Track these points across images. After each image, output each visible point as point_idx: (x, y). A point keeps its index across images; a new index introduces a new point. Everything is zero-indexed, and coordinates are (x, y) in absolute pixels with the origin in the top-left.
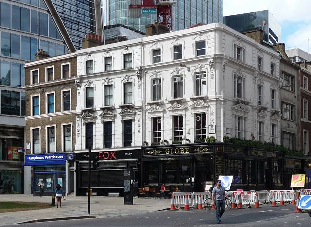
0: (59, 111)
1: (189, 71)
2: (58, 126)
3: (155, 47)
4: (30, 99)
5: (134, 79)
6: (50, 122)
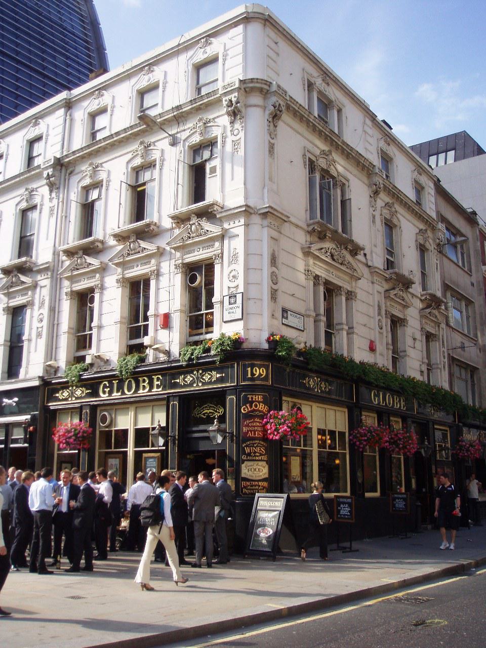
1: (174, 144)
5: (43, 191)
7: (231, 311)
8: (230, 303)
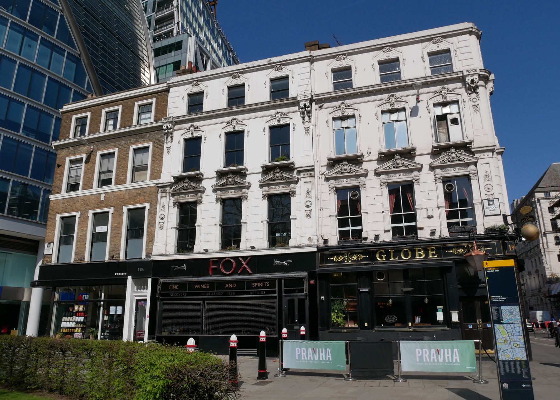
0: (124, 182)
4: (64, 165)
6: (100, 204)
7: (490, 209)
8: (489, 205)
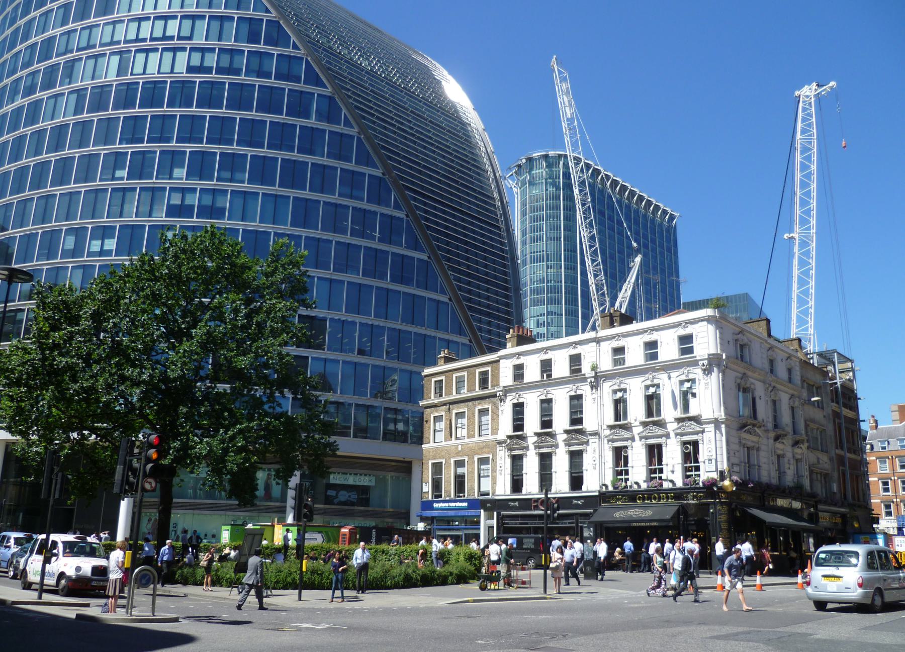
0: (473, 436)
2: (471, 458)
3: (616, 344)
6: (458, 453)
